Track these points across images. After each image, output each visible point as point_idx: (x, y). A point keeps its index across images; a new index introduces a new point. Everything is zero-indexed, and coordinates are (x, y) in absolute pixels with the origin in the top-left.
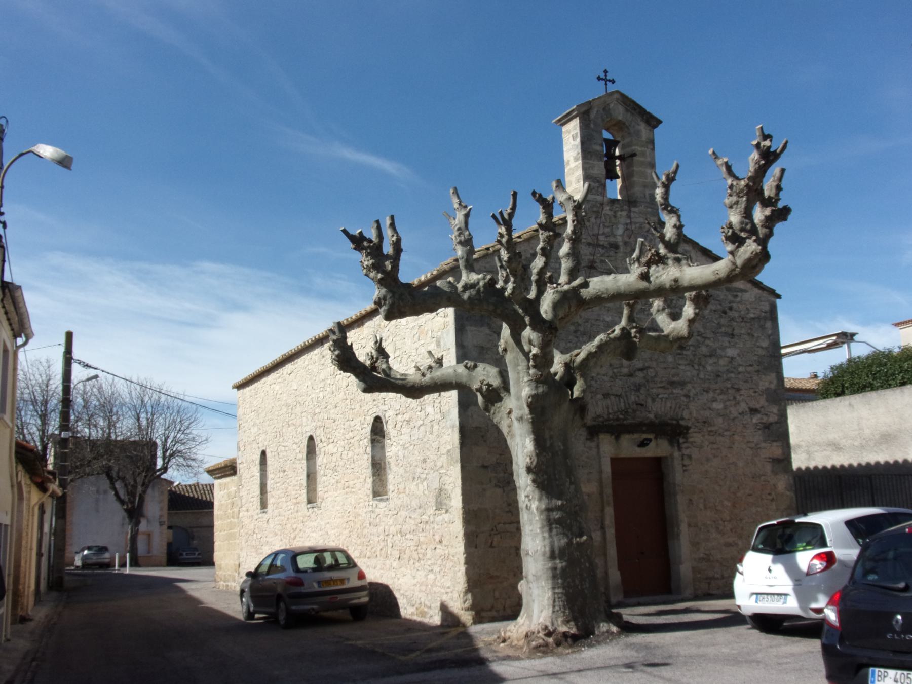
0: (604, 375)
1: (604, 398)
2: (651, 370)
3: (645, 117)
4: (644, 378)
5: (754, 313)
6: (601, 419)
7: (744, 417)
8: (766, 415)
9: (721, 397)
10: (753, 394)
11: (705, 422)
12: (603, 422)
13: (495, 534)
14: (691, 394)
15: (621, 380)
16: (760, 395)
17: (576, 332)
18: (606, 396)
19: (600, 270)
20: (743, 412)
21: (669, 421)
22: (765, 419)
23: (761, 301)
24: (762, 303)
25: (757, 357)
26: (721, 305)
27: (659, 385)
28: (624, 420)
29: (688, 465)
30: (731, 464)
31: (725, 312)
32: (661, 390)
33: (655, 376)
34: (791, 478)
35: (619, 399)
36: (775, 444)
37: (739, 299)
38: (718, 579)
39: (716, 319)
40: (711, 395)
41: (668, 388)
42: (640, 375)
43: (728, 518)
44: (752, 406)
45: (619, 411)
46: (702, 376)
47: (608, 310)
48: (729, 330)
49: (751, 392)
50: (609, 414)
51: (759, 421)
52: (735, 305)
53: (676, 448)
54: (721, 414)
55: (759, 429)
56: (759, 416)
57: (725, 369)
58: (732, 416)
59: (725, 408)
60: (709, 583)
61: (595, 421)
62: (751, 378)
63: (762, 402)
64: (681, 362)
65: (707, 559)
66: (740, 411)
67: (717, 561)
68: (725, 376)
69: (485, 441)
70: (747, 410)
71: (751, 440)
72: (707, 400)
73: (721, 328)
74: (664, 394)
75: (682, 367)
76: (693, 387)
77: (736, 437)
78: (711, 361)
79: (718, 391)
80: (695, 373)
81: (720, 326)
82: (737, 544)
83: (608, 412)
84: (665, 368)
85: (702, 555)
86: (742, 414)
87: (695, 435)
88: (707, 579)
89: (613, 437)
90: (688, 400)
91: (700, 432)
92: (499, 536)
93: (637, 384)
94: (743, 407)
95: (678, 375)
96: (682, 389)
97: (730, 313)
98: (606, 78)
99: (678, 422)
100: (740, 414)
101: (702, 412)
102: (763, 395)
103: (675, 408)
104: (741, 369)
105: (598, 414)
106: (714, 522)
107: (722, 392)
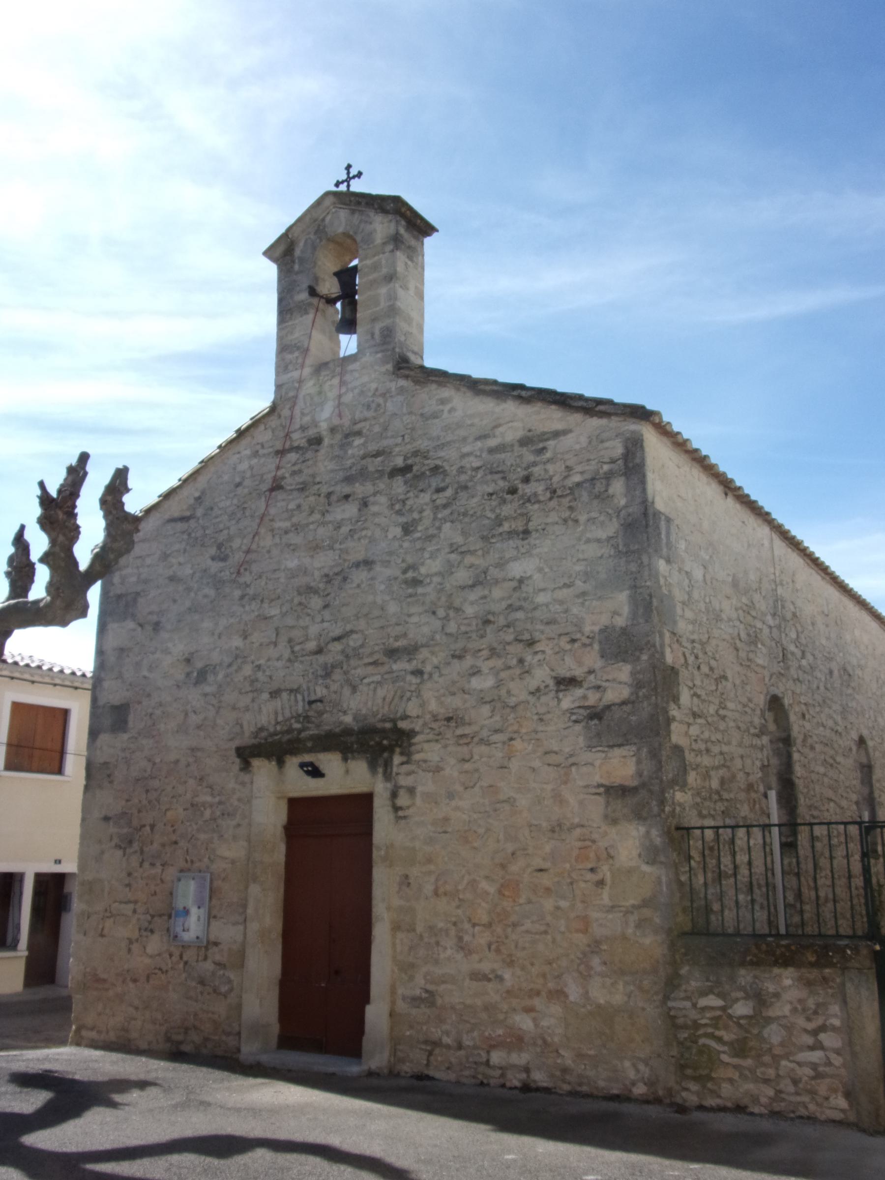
0: (278, 660)
1: (271, 697)
2: (354, 636)
3: (376, 206)
4: (343, 652)
5: (582, 473)
6: (264, 734)
7: (539, 698)
8: (598, 688)
9: (491, 663)
10: (568, 647)
11: (449, 719)
12: (266, 739)
13: (108, 917)
14: (428, 668)
15: (302, 662)
16: (585, 645)
17: (242, 597)
18: (275, 694)
19: (289, 488)
20: (538, 690)
21: (380, 725)
22: (593, 698)
23: (602, 442)
24: (607, 444)
25: (584, 563)
26: (504, 478)
27: (366, 661)
28: (300, 731)
29: (408, 807)
30: (504, 801)
31: (513, 491)
32: (370, 669)
33: (362, 646)
34: (654, 832)
35: (296, 696)
36: (617, 752)
37: (548, 455)
38: (448, 1047)
39: (493, 510)
40: (469, 661)
41: (382, 664)
42: (337, 647)
43: (485, 919)
44: (564, 673)
45: (292, 717)
46: (452, 627)
47: (294, 550)
48: (519, 525)
49: (564, 643)
50: (277, 723)
51: (577, 704)
52: (537, 470)
53: (380, 776)
54: (487, 699)
55: (576, 722)
56: (579, 692)
57: (504, 604)
58: (512, 701)
59: (499, 685)
60: (430, 1053)
61: (256, 737)
62: (566, 611)
63: (592, 658)
64: (413, 610)
65: (429, 999)
66: (532, 688)
67: (453, 1008)
68: (502, 621)
69: (111, 782)
70: (551, 683)
71: (556, 749)
72: (459, 673)
73: (500, 525)
74: (376, 674)
75: (415, 619)
76: (433, 653)
77: (517, 744)
78: (473, 596)
79: (485, 653)
80: (438, 624)
81: (499, 521)
82: (500, 979)
83: (276, 719)
84: (382, 627)
85: (417, 992)
86: (536, 692)
87: (426, 746)
88: (426, 1042)
89: (274, 763)
90: (418, 681)
91: (437, 741)
92: (112, 920)
93: (329, 665)
94: (541, 676)
95: (405, 635)
96: (409, 661)
97: (527, 489)
98: (346, 181)
99: (395, 725)
100: (532, 693)
101: (449, 700)
102: (591, 645)
103: (393, 699)
104: (541, 598)
105: (259, 726)
106: (455, 924)
107: (493, 653)
